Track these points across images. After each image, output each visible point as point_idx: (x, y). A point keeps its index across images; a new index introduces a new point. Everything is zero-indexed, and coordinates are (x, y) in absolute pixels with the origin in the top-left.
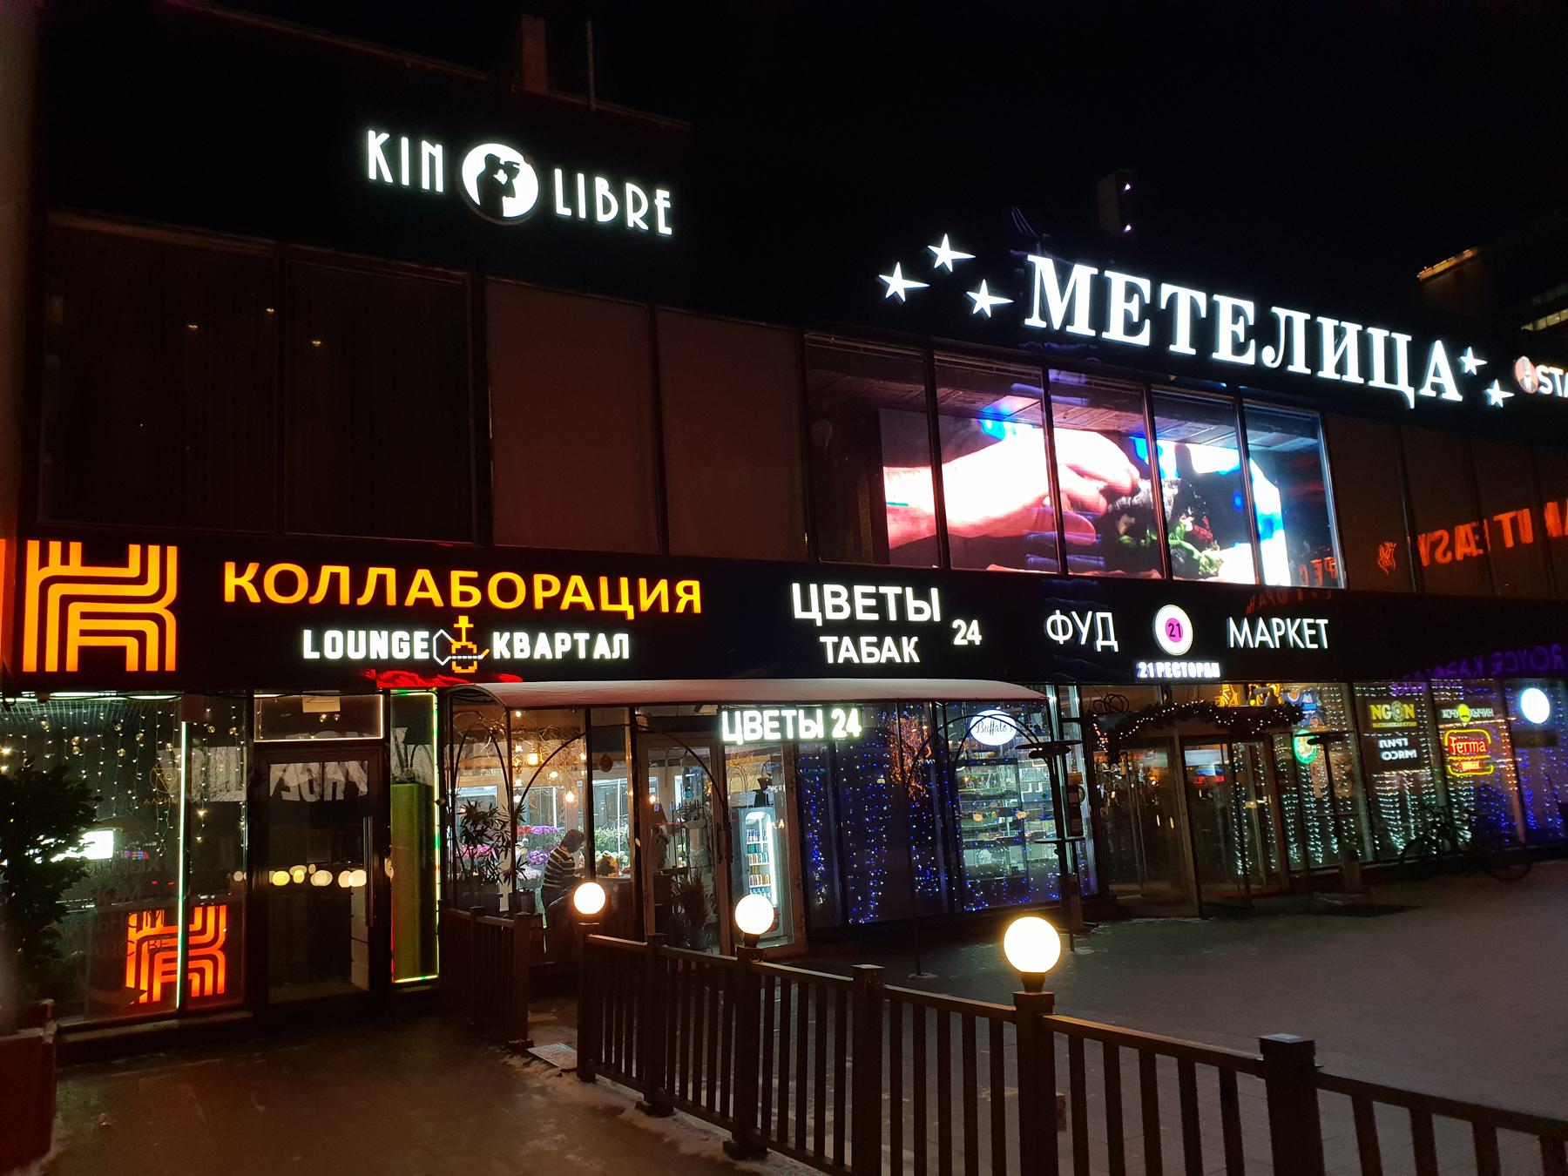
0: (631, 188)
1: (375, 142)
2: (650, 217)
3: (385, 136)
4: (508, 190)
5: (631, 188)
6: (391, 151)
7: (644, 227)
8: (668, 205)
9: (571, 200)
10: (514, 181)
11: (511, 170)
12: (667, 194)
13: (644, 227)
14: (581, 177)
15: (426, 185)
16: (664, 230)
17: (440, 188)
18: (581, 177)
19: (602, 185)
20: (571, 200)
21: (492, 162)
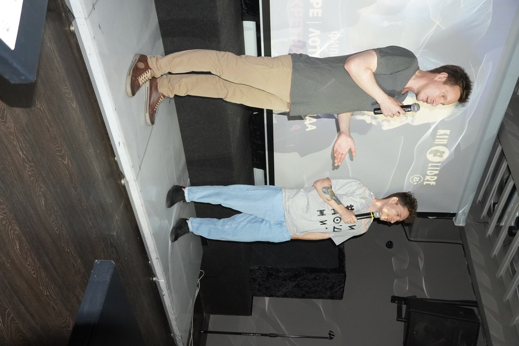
0: (436, 178)
1: (448, 132)
2: (428, 180)
3: (448, 133)
4: (435, 155)
5: (436, 178)
6: (446, 134)
7: (426, 179)
9: (432, 166)
11: (441, 156)
13: (426, 179)
15: (436, 140)
16: (425, 183)
17: (436, 143)
19: (437, 172)
21: (444, 152)
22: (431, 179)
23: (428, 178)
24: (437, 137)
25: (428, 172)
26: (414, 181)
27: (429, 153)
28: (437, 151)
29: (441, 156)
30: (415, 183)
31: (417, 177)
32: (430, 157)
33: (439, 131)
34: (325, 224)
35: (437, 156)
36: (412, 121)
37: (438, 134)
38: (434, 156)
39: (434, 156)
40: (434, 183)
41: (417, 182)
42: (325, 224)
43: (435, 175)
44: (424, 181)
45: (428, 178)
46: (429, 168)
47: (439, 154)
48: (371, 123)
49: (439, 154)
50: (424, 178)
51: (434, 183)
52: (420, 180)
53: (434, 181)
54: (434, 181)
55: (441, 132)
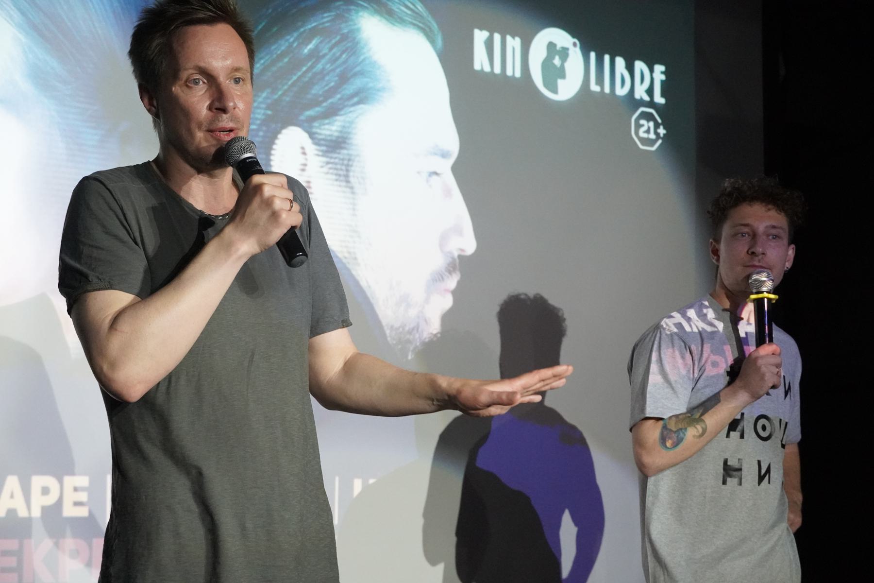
2: (650, 91)
5: (639, 65)
7: (647, 98)
8: (663, 77)
9: (600, 81)
10: (567, 65)
11: (564, 53)
12: (662, 68)
13: (647, 98)
14: (607, 58)
15: (509, 73)
16: (659, 99)
17: (518, 74)
18: (607, 58)
19: (620, 62)
20: (600, 81)
22: (647, 80)
23: (640, 93)
24: (497, 70)
25: (622, 91)
26: (652, 136)
27: (555, 91)
28: (547, 65)
29: (564, 53)
30: (662, 131)
31: (638, 126)
32: (567, 89)
33: (477, 67)
34: (768, 470)
35: (562, 66)
36: (445, 155)
37: (487, 69)
38: (563, 76)
39: (563, 76)
40: (659, 69)
41: (657, 126)
42: (768, 470)
43: (630, 68)
44: (651, 104)
45: (640, 93)
46: (607, 90)
47: (557, 61)
48: (454, 293)
49: (557, 61)
50: (641, 103)
51: (659, 69)
52: (649, 117)
53: (652, 71)
54: (652, 71)
55: (480, 61)
